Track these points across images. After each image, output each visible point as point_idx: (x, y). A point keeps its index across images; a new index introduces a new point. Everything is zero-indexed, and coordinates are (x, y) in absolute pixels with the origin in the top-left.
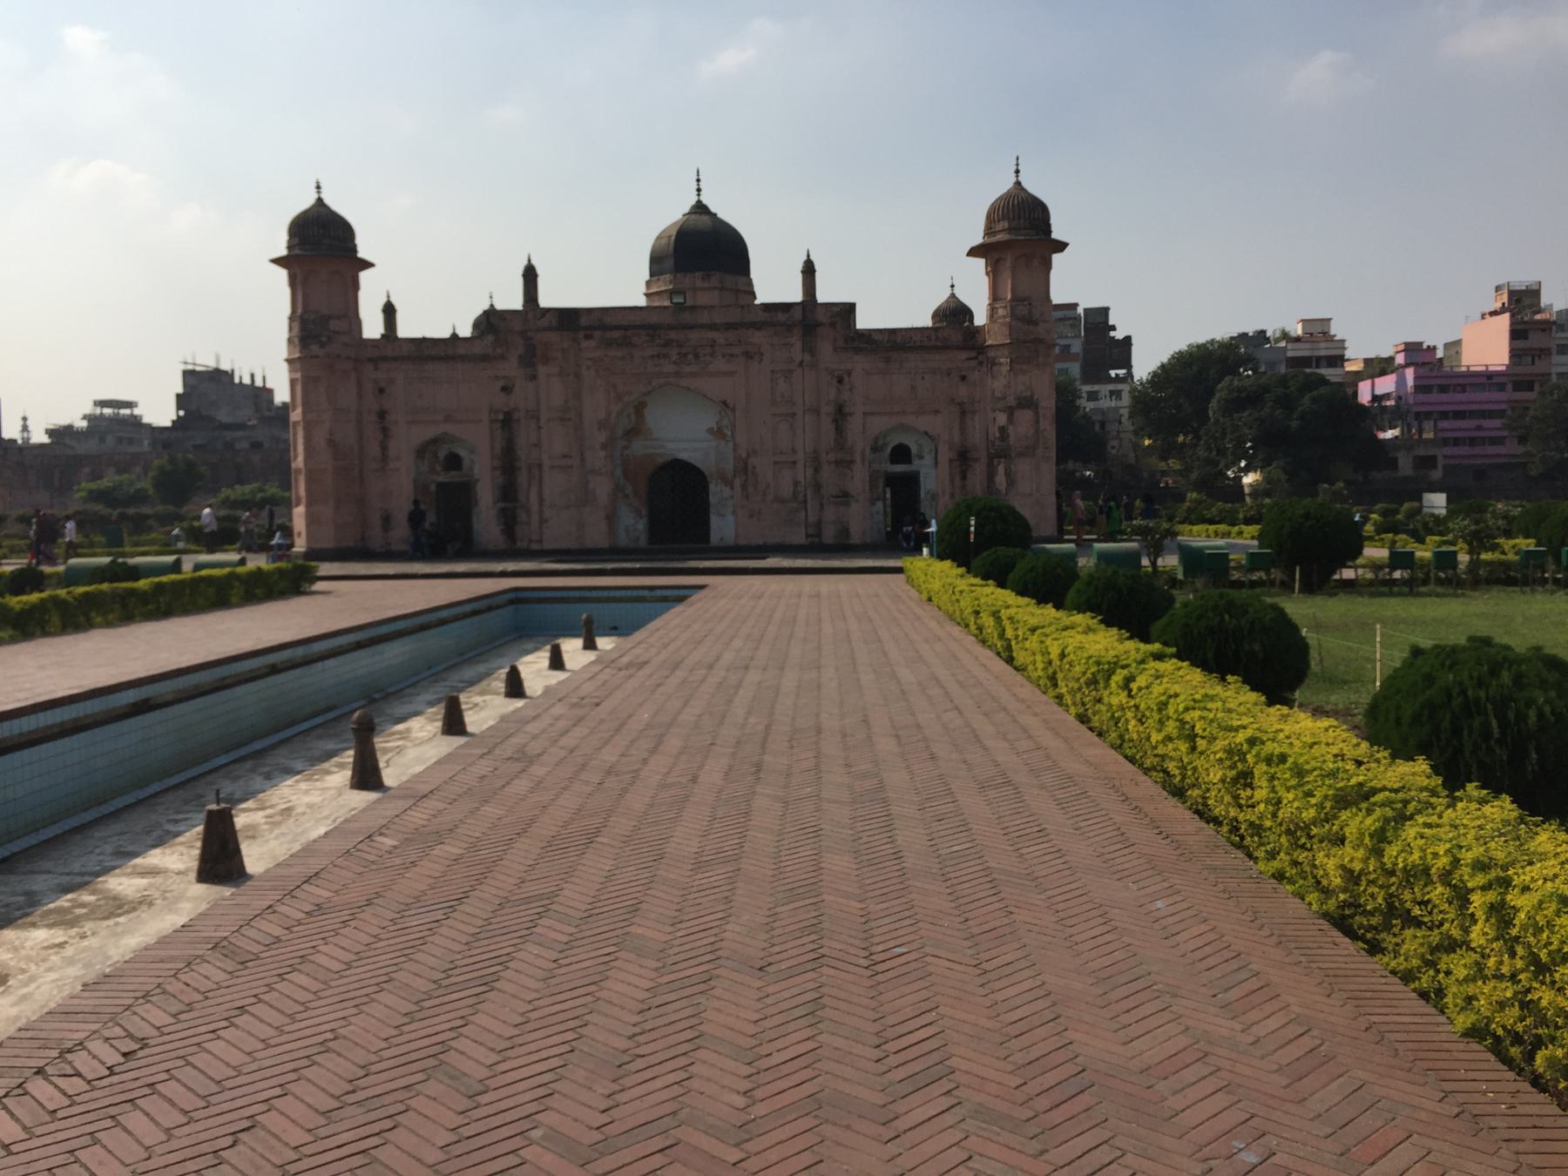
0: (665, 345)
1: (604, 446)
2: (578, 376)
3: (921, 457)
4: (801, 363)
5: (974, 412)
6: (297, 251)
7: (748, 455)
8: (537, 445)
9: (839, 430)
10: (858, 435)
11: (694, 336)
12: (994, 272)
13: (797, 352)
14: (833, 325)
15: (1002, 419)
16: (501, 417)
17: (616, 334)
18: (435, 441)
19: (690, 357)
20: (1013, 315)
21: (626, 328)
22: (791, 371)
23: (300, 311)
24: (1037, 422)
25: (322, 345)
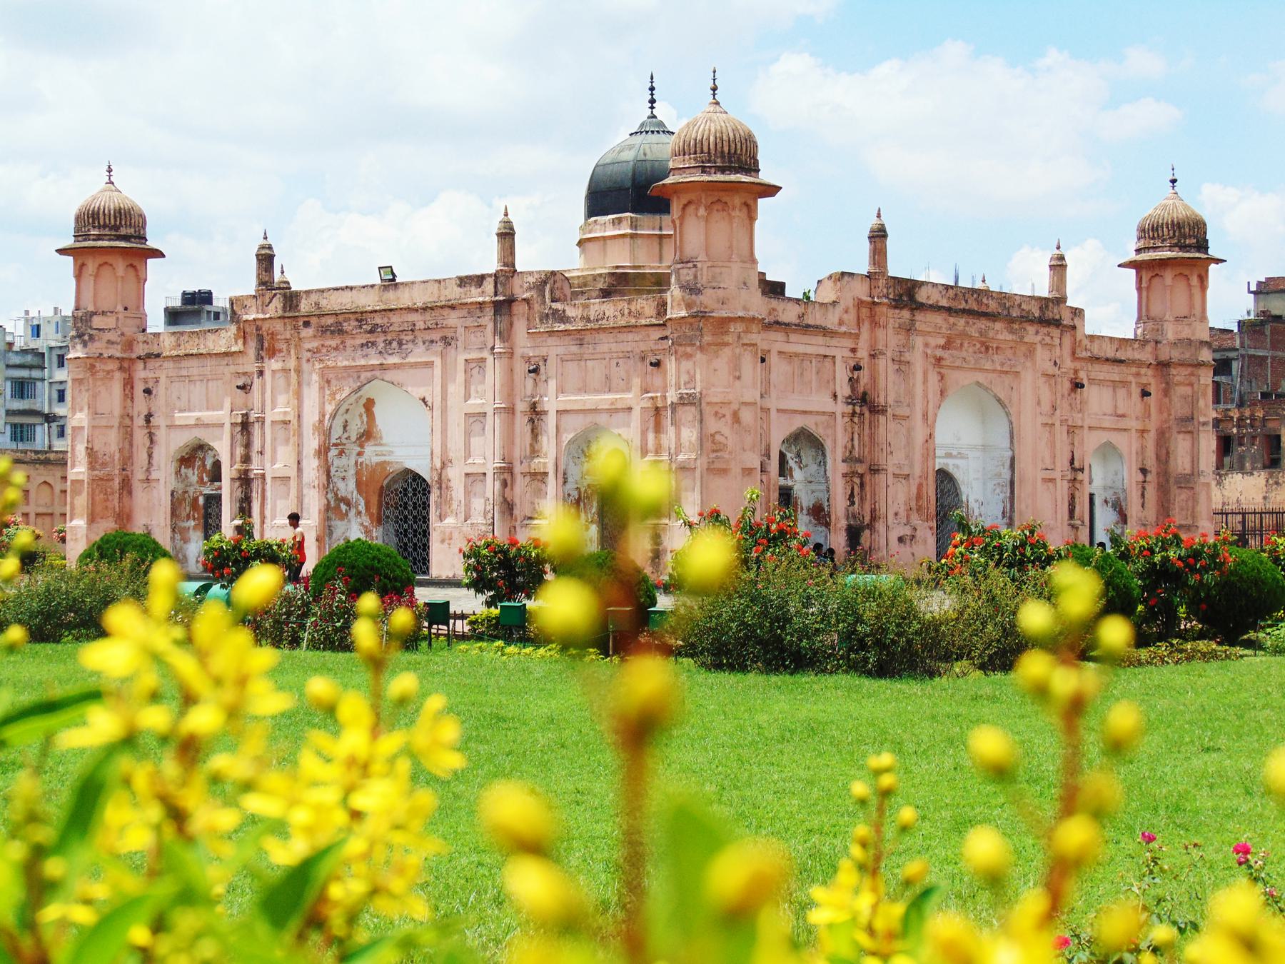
0: (371, 332)
11: (395, 318)
19: (395, 344)
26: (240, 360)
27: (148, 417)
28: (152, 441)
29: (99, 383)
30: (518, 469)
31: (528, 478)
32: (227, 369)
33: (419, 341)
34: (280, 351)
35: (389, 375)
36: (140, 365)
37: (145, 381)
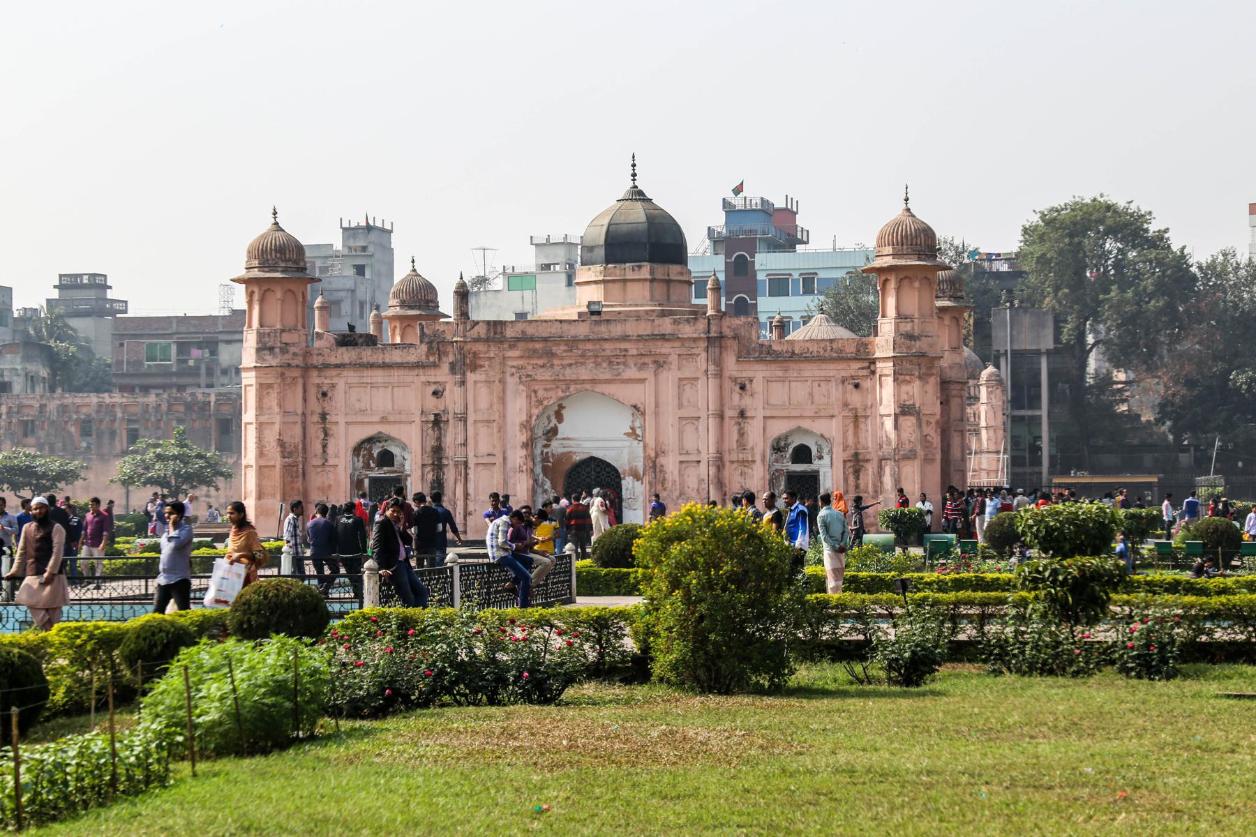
0: (583, 356)
1: (525, 445)
2: (502, 381)
3: (821, 458)
5: (866, 417)
6: (256, 273)
7: (657, 456)
8: (465, 444)
11: (607, 346)
16: (432, 418)
17: (538, 346)
18: (370, 440)
21: (545, 340)
22: (697, 379)
26: (432, 372)
28: (326, 434)
30: (727, 458)
33: (631, 362)
34: (481, 366)
35: (599, 388)
37: (318, 386)
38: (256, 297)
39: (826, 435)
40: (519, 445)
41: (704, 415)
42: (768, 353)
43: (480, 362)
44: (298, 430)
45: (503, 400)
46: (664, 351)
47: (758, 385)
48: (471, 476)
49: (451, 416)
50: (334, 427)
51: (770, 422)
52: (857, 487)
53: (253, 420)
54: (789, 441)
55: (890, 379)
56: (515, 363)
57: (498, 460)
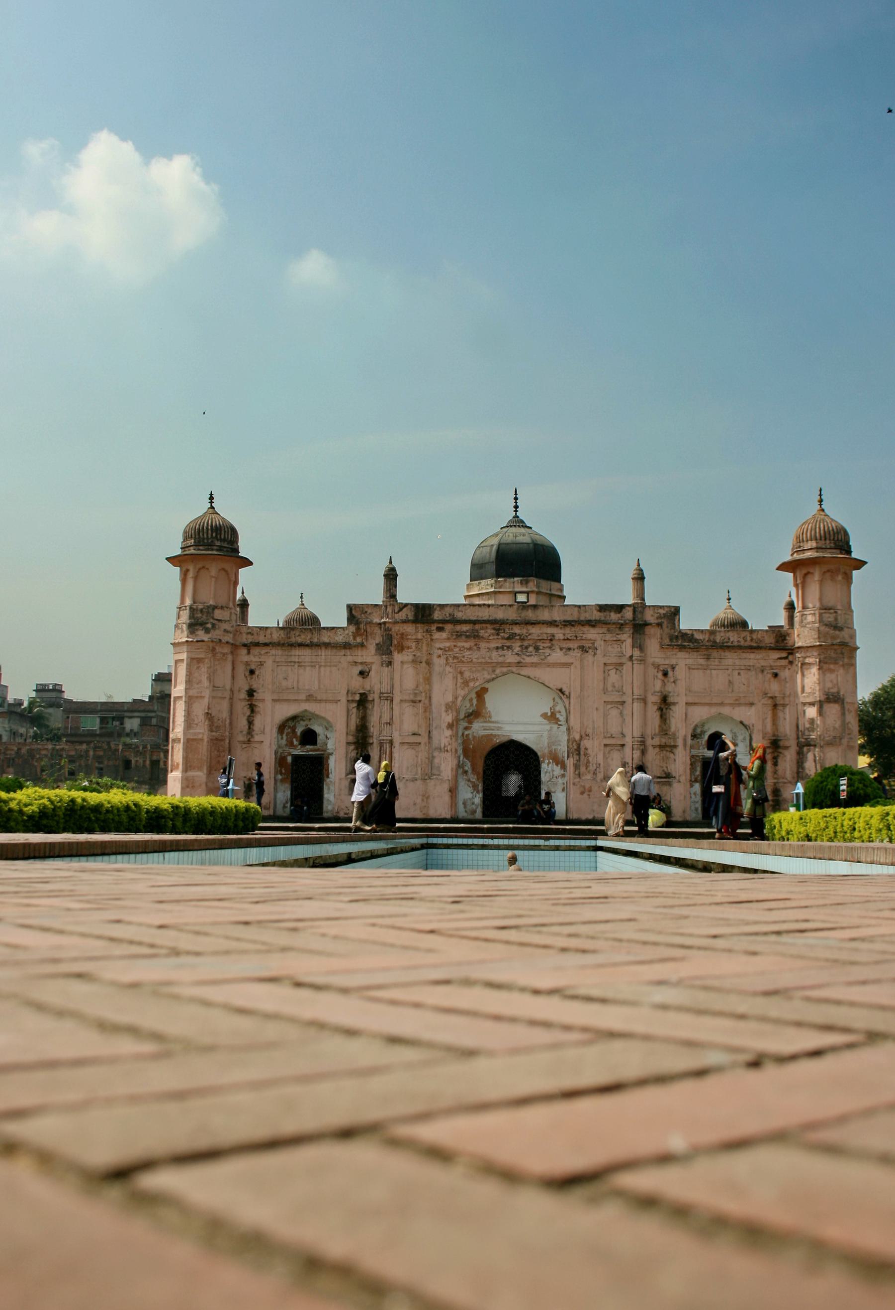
0: (508, 638)
1: (450, 726)
2: (428, 663)
4: (631, 657)
5: (784, 705)
6: (192, 551)
9: (664, 718)
10: (680, 724)
11: (535, 631)
12: (801, 585)
13: (627, 647)
14: (659, 625)
15: (812, 712)
16: (357, 697)
17: (465, 628)
18: (294, 718)
19: (531, 649)
20: (821, 621)
21: (474, 622)
22: (621, 664)
23: (188, 602)
24: (843, 714)
25: (207, 631)
26: (359, 652)
27: (251, 693)
28: (252, 711)
29: (217, 663)
30: (649, 742)
31: (657, 750)
32: (344, 659)
34: (409, 648)
35: (525, 671)
36: (244, 651)
37: (247, 664)
38: (191, 574)
39: (746, 723)
40: (444, 726)
41: (629, 700)
42: (690, 641)
43: (406, 643)
44: (225, 705)
45: (428, 680)
46: (589, 636)
47: (681, 672)
48: (396, 755)
49: (376, 696)
50: (260, 704)
51: (691, 709)
52: (775, 772)
53: (183, 694)
54: (706, 728)
55: (814, 670)
56: (442, 646)
57: (423, 739)
